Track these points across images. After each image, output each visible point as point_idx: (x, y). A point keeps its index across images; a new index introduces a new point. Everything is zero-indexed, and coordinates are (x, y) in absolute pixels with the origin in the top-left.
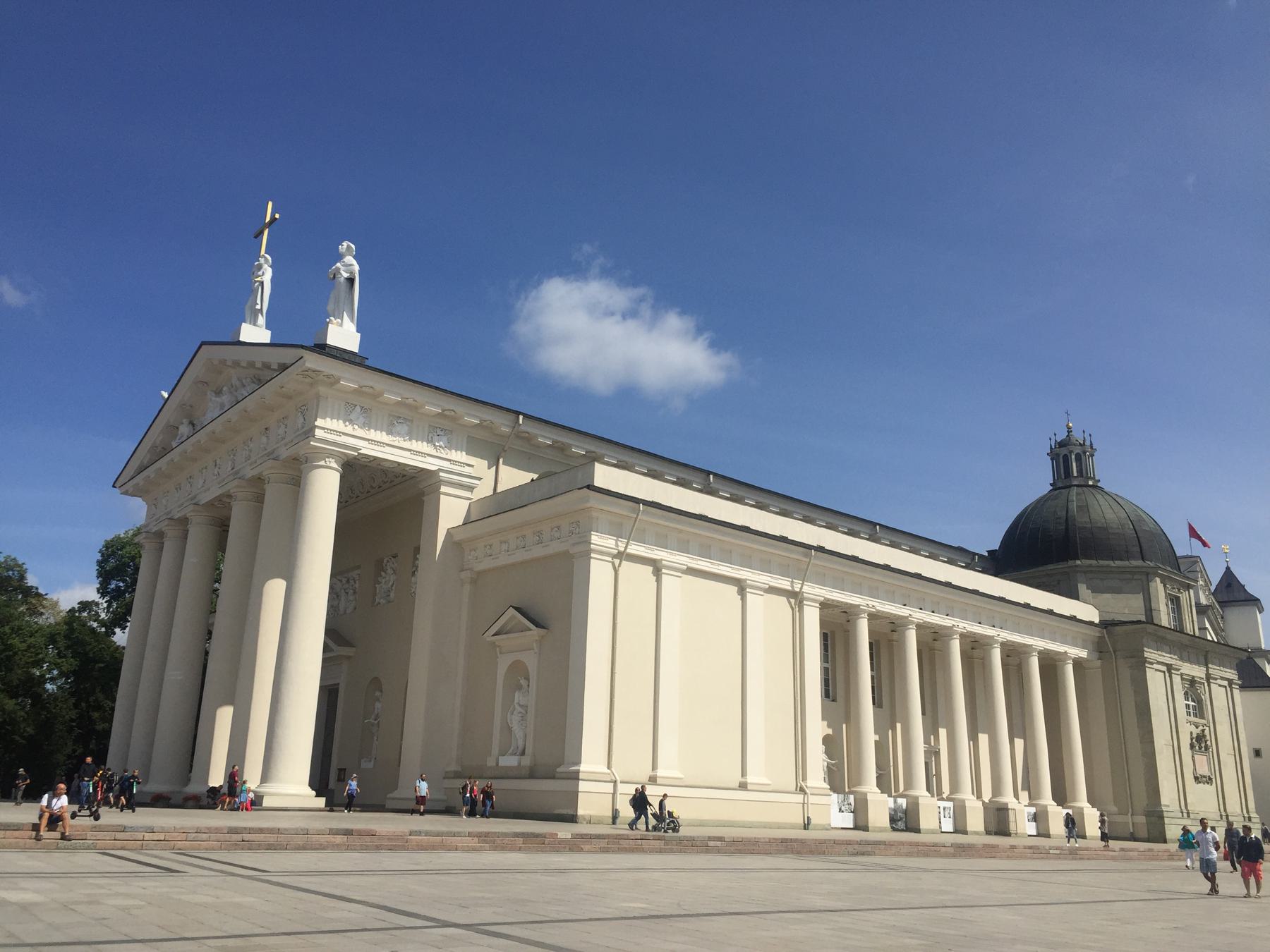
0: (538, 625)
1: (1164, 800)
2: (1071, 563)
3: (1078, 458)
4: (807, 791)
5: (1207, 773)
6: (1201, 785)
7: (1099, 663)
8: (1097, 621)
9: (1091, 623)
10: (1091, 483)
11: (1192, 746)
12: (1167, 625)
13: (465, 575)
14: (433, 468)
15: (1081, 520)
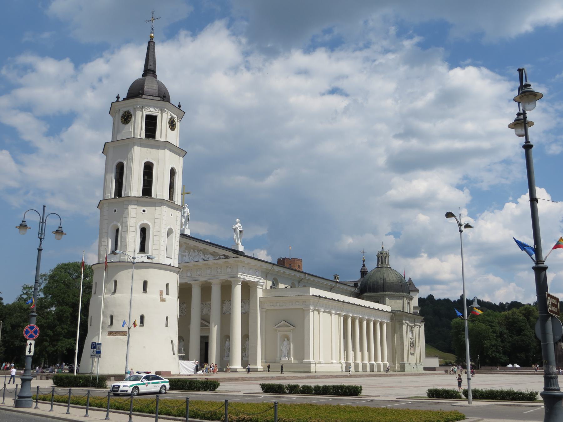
0: (294, 326)
1: (405, 361)
2: (384, 293)
3: (385, 258)
4: (342, 363)
5: (413, 352)
6: (412, 356)
7: (391, 323)
8: (391, 311)
9: (390, 312)
10: (388, 266)
11: (411, 345)
12: (407, 311)
13: (263, 310)
14: (256, 281)
15: (388, 280)
